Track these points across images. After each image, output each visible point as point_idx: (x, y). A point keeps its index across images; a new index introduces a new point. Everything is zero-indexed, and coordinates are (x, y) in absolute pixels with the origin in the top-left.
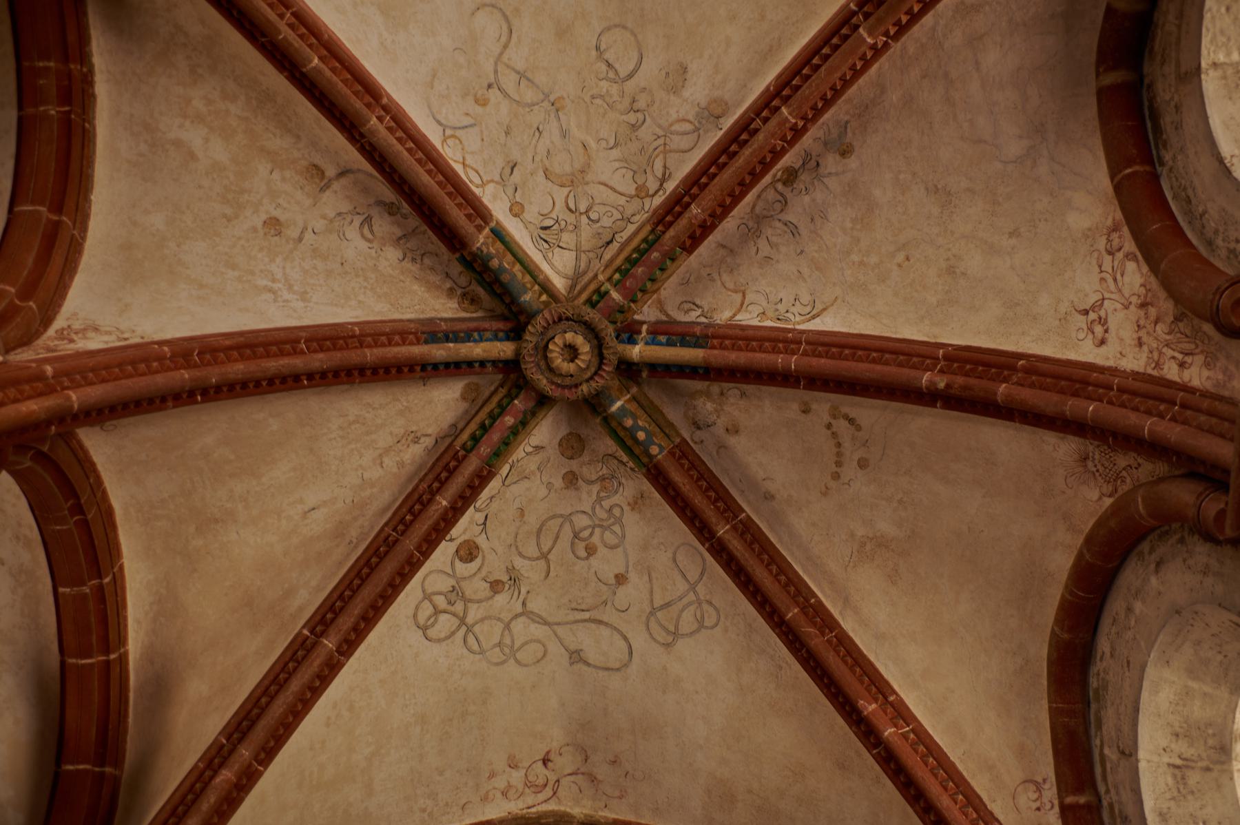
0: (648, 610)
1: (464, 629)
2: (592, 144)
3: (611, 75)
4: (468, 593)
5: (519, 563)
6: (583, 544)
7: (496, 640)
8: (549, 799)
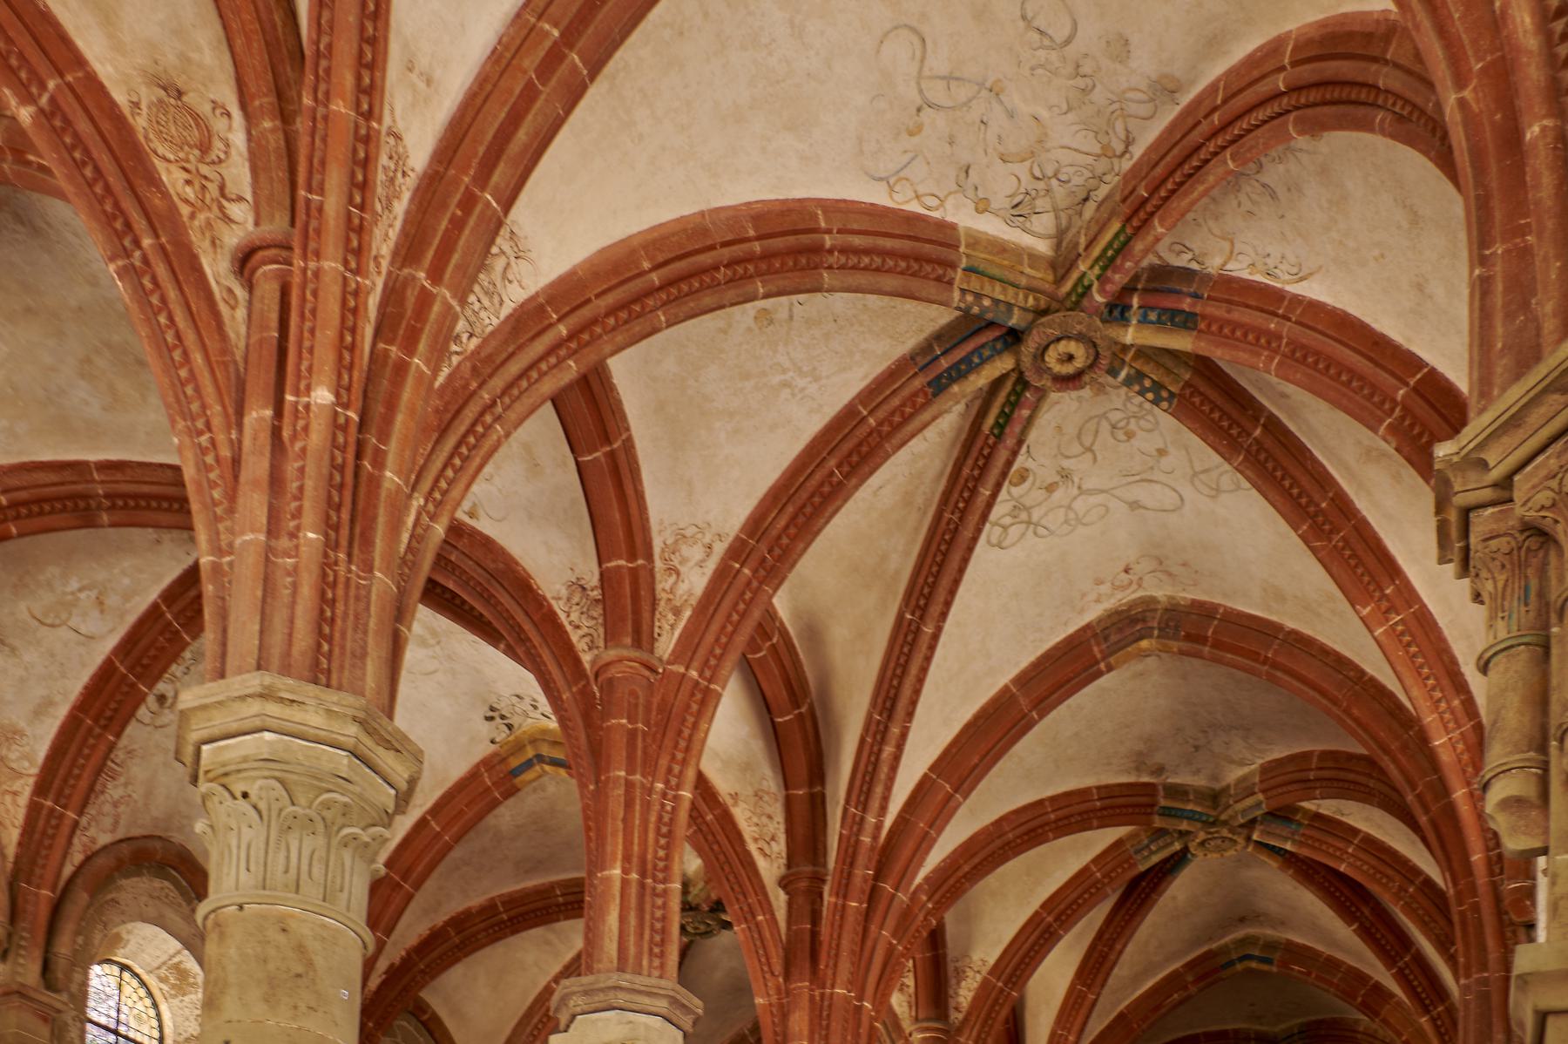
0: (1191, 472)
7: (1062, 519)
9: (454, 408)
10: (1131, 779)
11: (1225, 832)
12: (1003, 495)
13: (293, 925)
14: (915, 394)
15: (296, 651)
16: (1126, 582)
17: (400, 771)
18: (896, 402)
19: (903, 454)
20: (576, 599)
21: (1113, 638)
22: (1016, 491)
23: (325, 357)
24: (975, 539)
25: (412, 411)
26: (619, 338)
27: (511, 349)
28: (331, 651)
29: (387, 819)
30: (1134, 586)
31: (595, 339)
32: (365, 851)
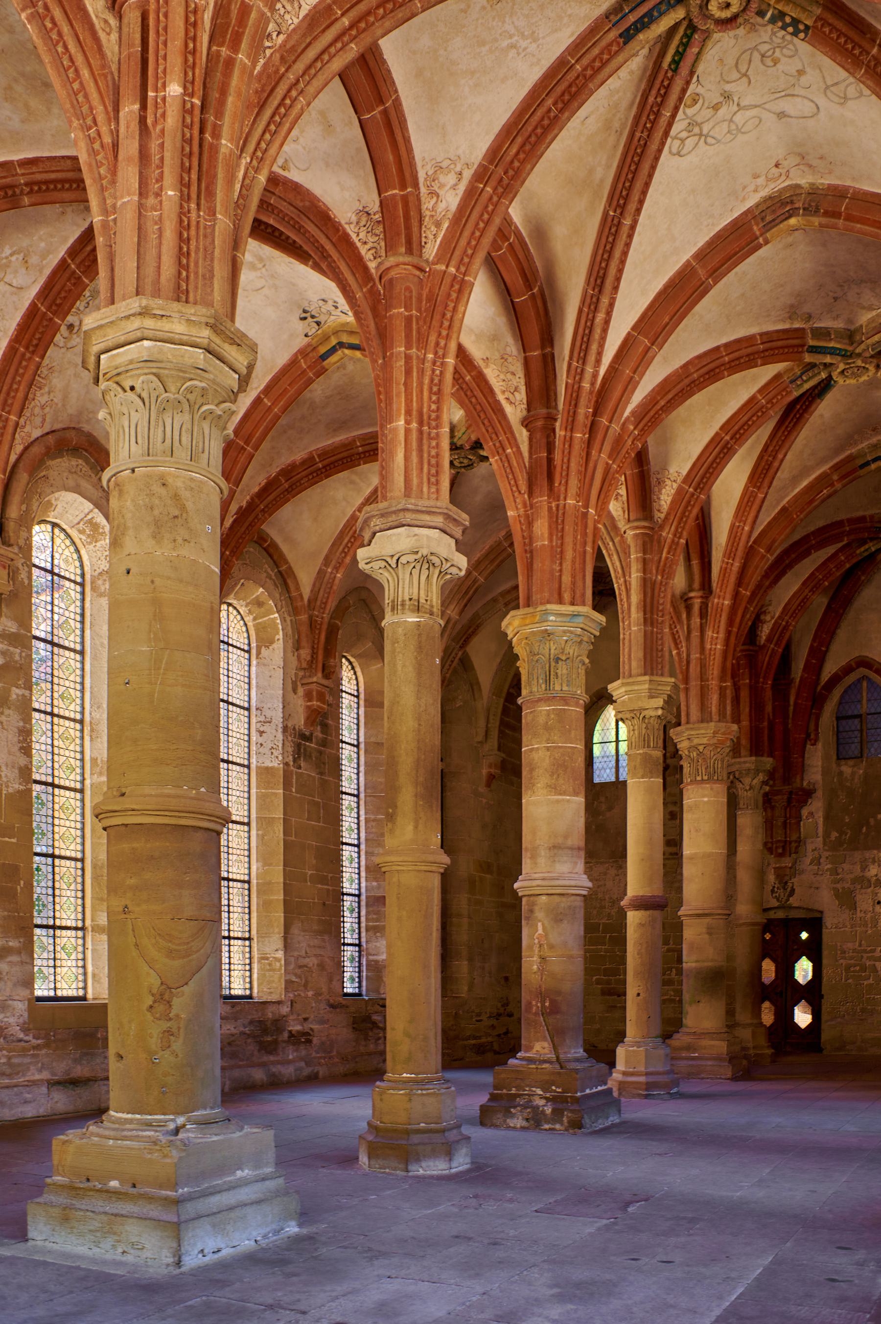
4: (699, 121)
5: (728, 87)
9: (268, 89)
10: (787, 326)
11: (859, 363)
12: (680, 115)
13: (170, 480)
14: (610, 44)
15: (163, 279)
16: (776, 175)
17: (240, 359)
18: (596, 51)
19: (602, 92)
20: (363, 223)
21: (769, 218)
22: (690, 112)
23: (175, 61)
24: (660, 151)
25: (239, 94)
26: (387, 24)
27: (308, 40)
28: (188, 277)
29: (234, 396)
30: (783, 177)
31: (369, 26)
32: (219, 421)
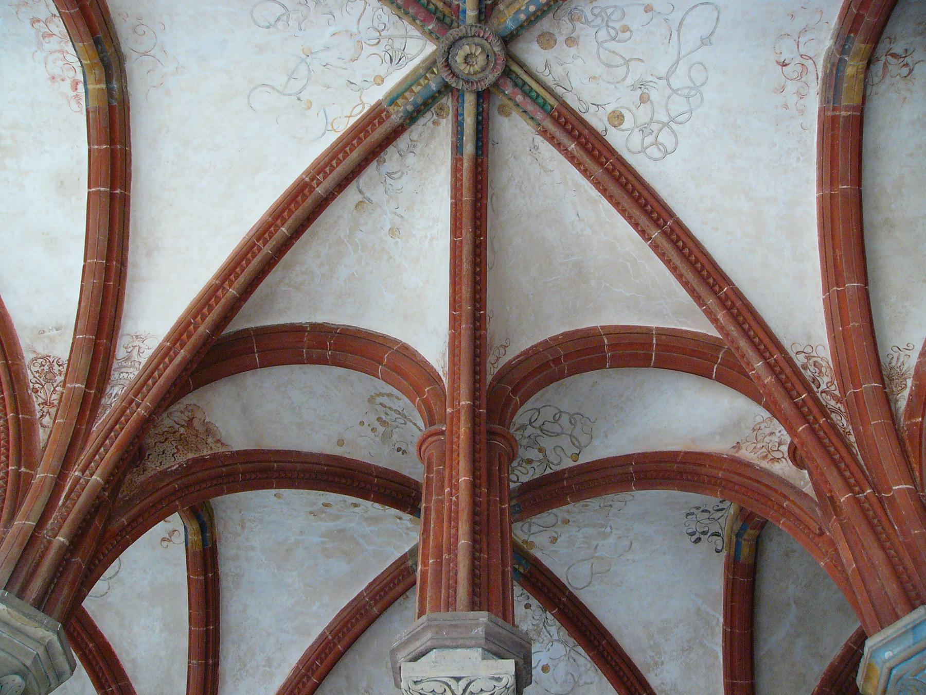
1: (671, 124)
2: (332, 29)
3: (285, 18)
4: (647, 120)
5: (629, 81)
6: (620, 34)
8: (814, 63)
